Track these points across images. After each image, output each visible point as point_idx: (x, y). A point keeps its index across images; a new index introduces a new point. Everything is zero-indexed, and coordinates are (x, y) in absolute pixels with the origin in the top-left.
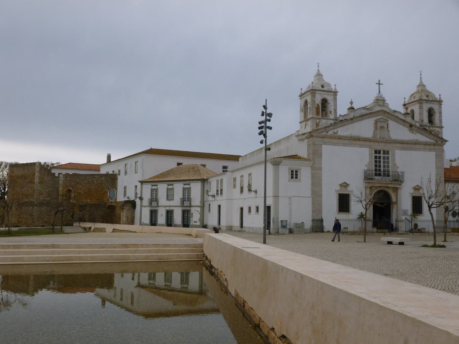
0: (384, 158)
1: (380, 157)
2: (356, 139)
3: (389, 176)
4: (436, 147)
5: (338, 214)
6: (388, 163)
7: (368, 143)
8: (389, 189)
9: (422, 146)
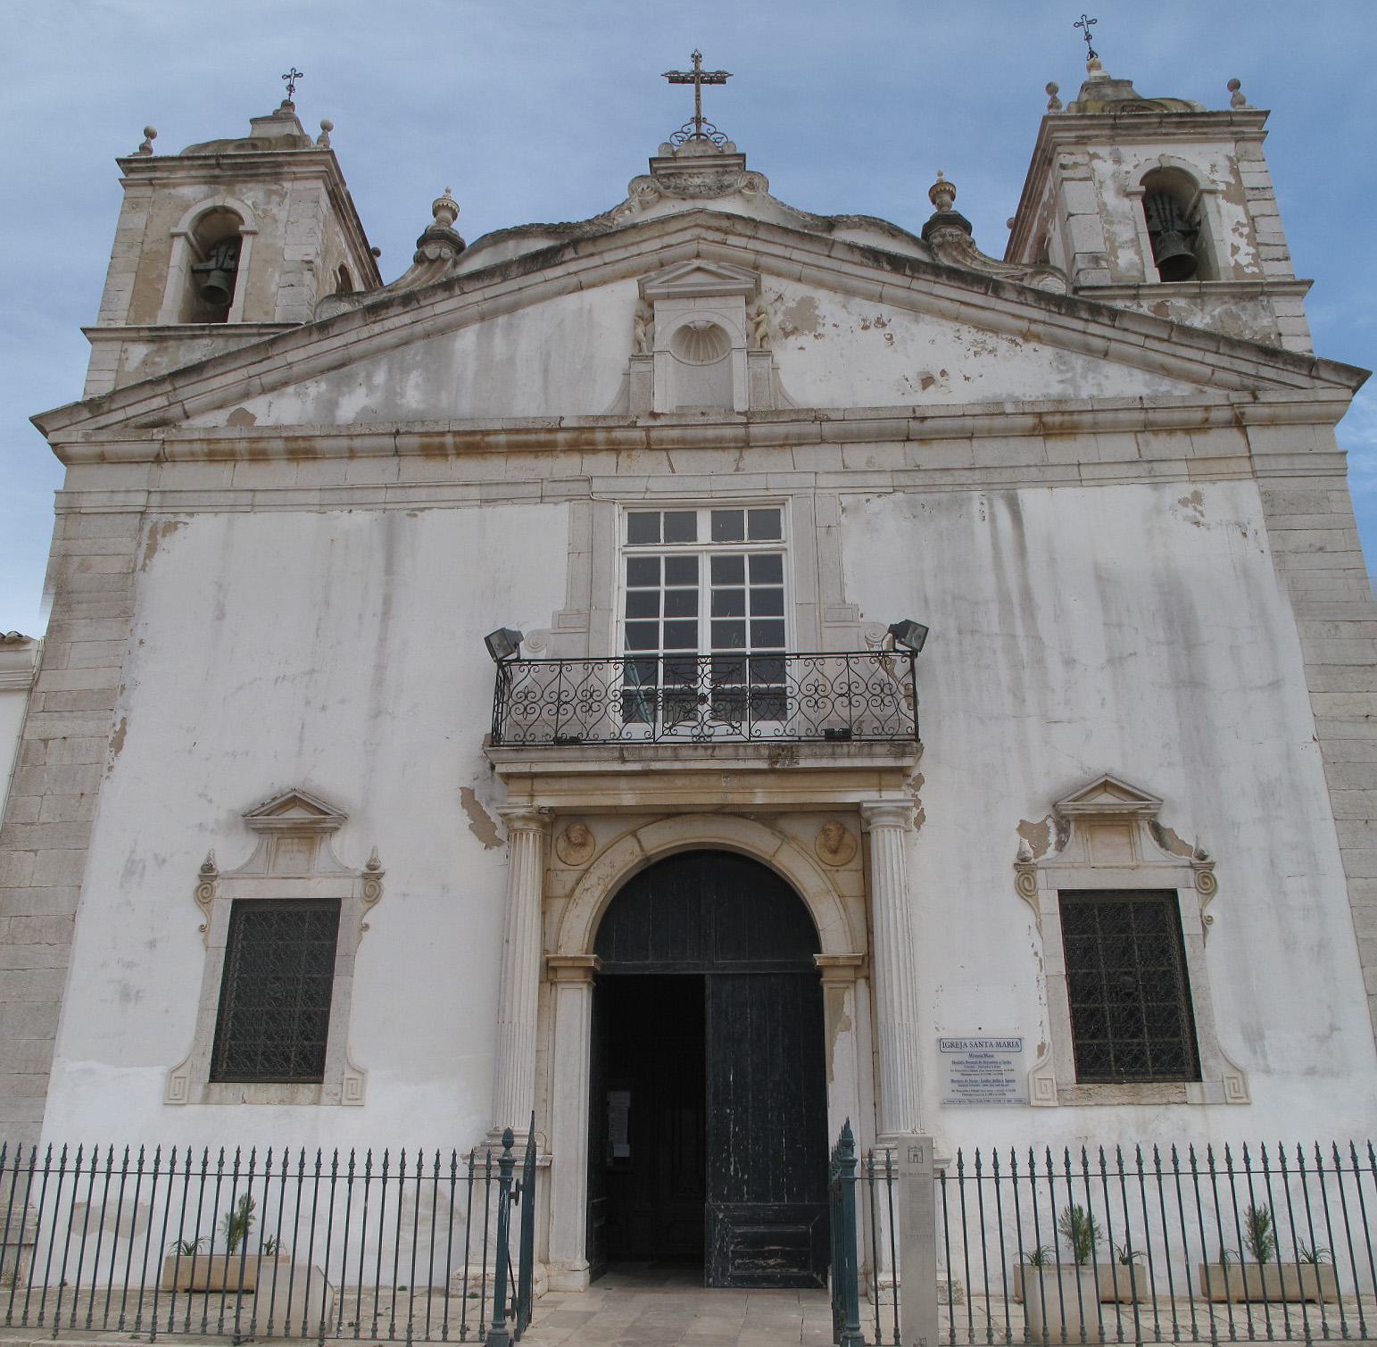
0: (726, 569)
1: (684, 569)
2: (449, 440)
3: (774, 704)
5: (206, 1100)
6: (771, 602)
7: (567, 465)
8: (784, 836)
9: (1124, 446)
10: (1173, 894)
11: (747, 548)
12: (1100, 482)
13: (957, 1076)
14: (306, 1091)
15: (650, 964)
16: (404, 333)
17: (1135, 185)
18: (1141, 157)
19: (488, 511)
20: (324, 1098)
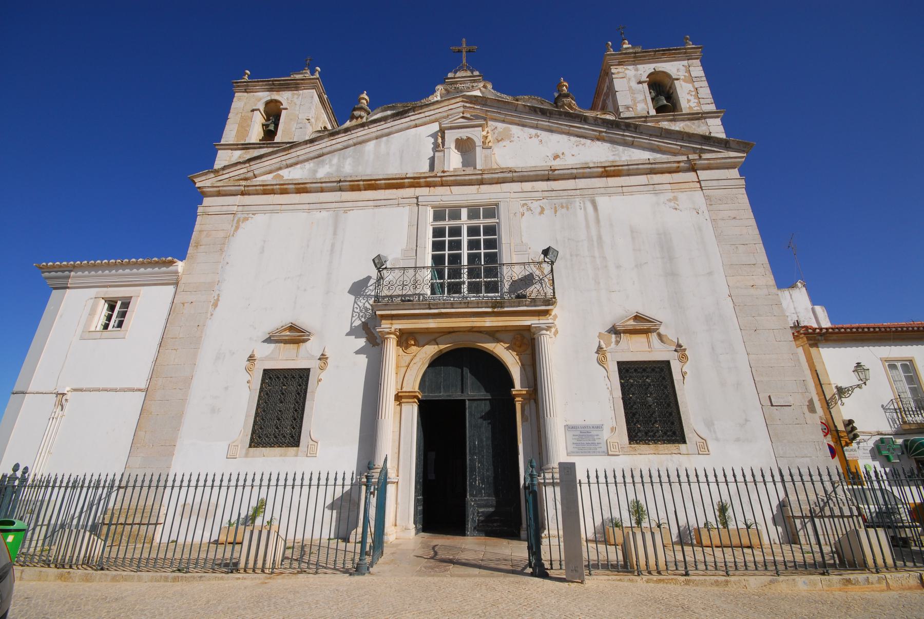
0: (473, 231)
1: (456, 231)
4: (703, 174)
5: (246, 455)
10: (668, 363)
11: (482, 222)
12: (631, 193)
13: (575, 441)
14: (292, 450)
15: (442, 395)
16: (345, 144)
17: (644, 78)
18: (645, 69)
19: (377, 210)
20: (300, 453)
